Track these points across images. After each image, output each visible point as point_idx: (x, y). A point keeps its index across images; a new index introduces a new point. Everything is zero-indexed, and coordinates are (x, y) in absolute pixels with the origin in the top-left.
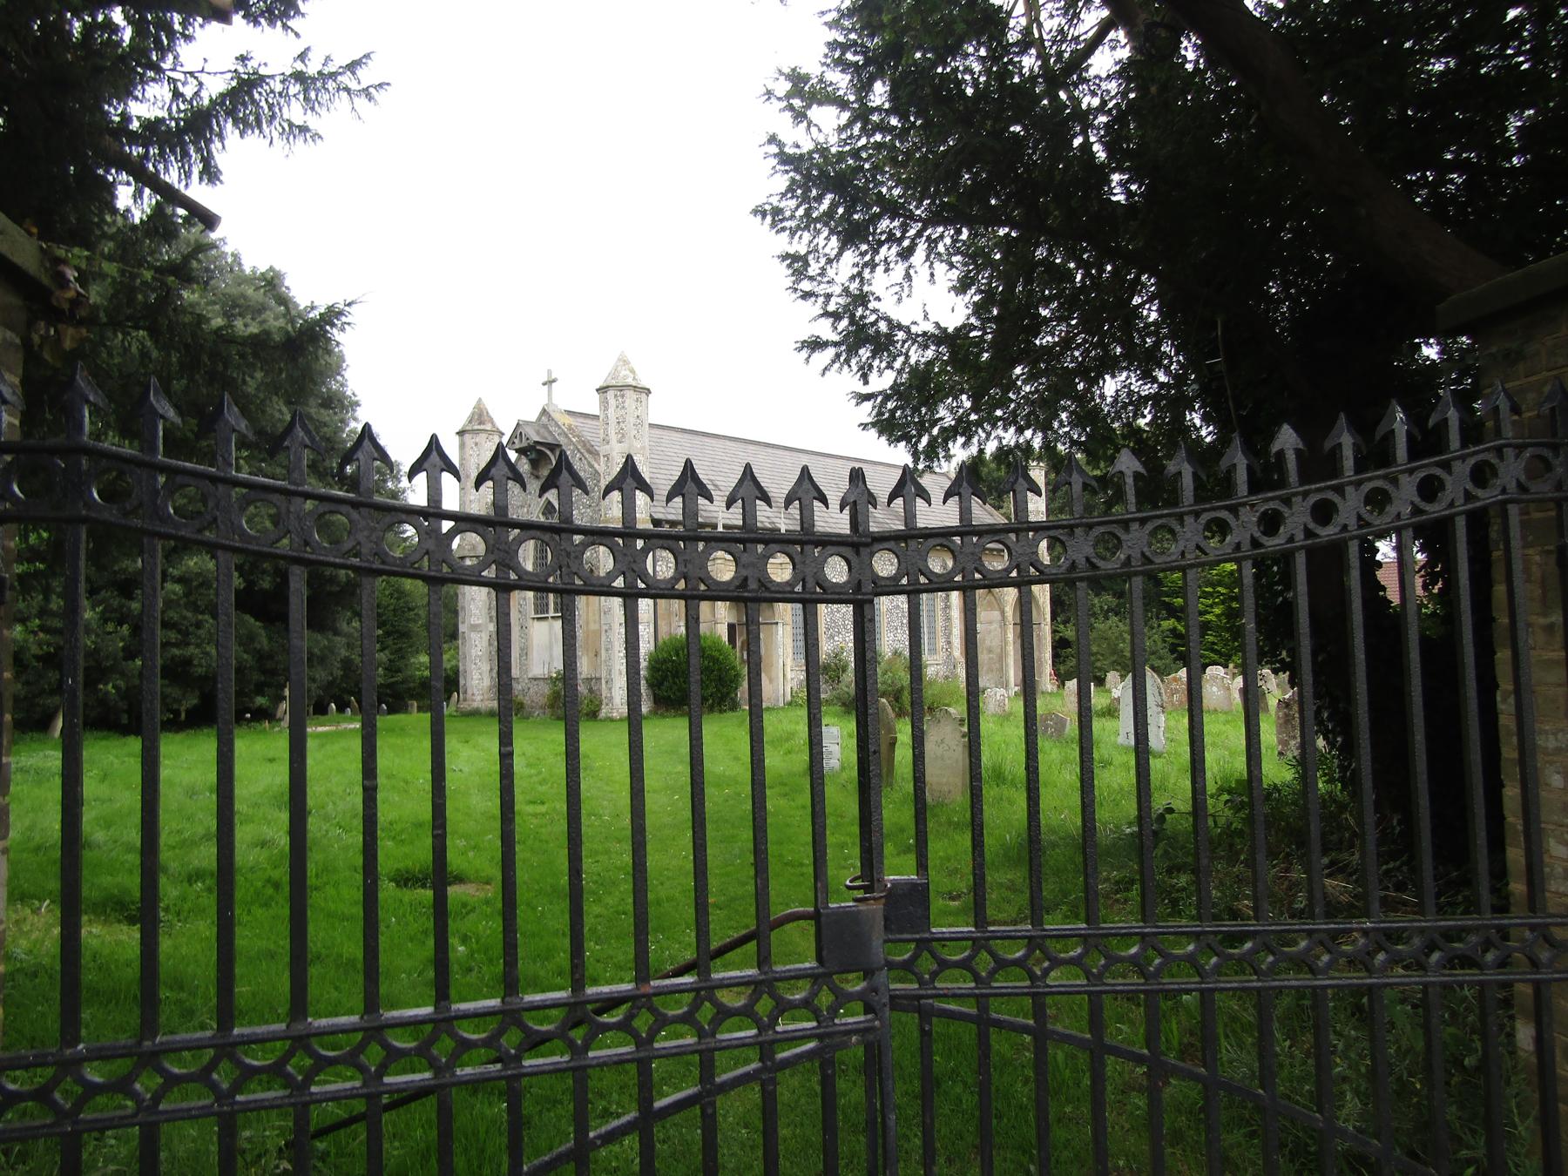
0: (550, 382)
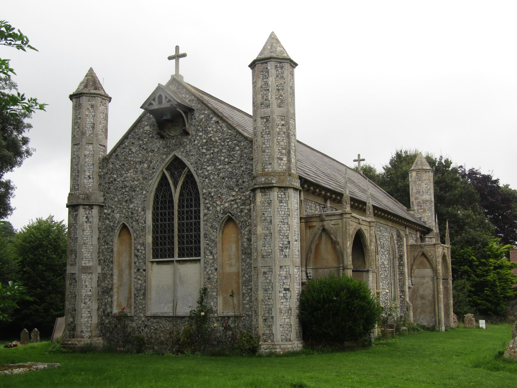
0: (177, 56)
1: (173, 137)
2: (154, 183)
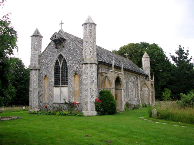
1: (60, 48)
2: (54, 62)
